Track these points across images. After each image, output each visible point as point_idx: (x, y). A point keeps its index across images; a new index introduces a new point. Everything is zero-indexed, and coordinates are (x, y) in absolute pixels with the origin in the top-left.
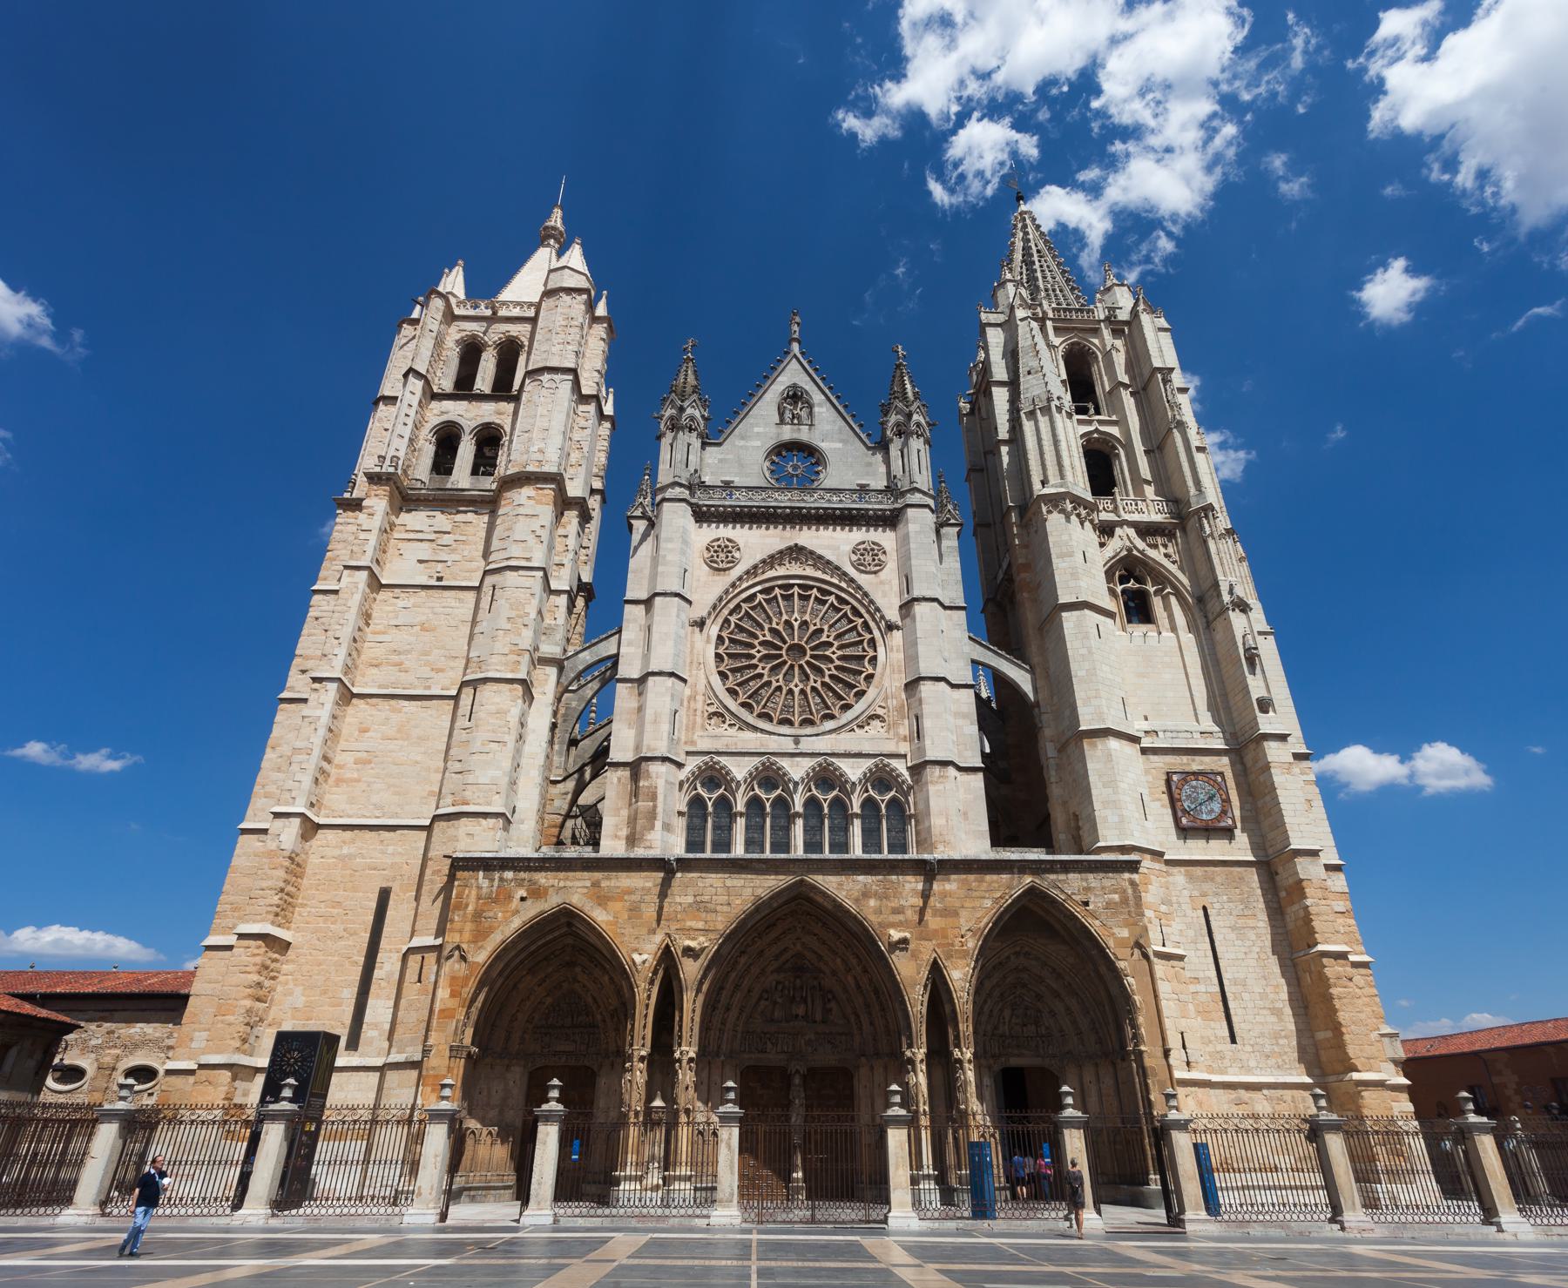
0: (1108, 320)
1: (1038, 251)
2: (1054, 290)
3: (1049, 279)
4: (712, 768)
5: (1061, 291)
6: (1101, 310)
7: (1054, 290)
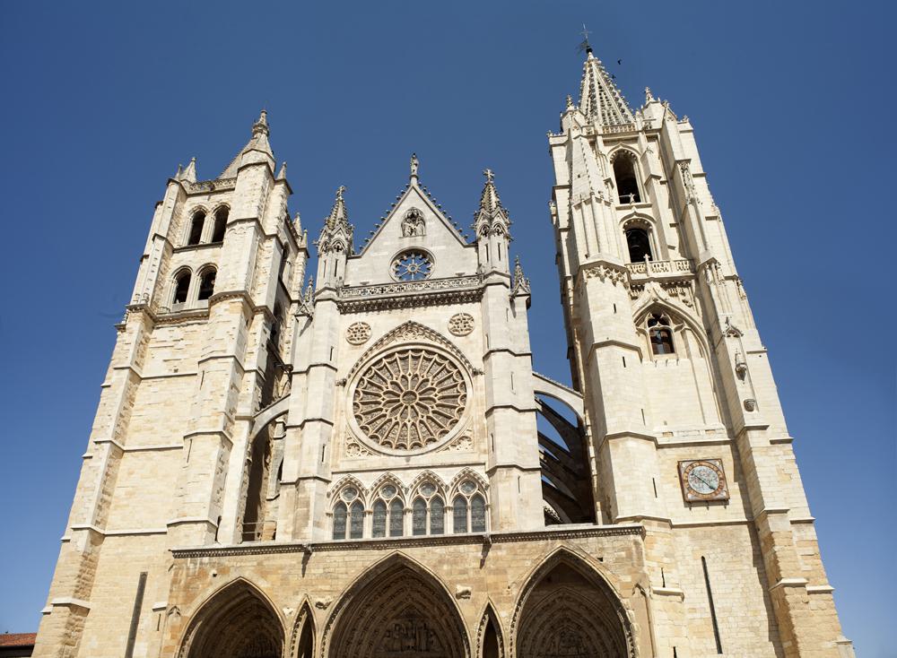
0: (645, 130)
1: (600, 87)
2: (609, 114)
3: (606, 106)
4: (468, 475)
5: (614, 114)
6: (639, 123)
7: (609, 114)
